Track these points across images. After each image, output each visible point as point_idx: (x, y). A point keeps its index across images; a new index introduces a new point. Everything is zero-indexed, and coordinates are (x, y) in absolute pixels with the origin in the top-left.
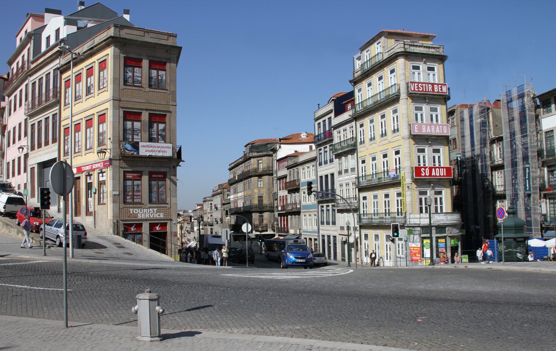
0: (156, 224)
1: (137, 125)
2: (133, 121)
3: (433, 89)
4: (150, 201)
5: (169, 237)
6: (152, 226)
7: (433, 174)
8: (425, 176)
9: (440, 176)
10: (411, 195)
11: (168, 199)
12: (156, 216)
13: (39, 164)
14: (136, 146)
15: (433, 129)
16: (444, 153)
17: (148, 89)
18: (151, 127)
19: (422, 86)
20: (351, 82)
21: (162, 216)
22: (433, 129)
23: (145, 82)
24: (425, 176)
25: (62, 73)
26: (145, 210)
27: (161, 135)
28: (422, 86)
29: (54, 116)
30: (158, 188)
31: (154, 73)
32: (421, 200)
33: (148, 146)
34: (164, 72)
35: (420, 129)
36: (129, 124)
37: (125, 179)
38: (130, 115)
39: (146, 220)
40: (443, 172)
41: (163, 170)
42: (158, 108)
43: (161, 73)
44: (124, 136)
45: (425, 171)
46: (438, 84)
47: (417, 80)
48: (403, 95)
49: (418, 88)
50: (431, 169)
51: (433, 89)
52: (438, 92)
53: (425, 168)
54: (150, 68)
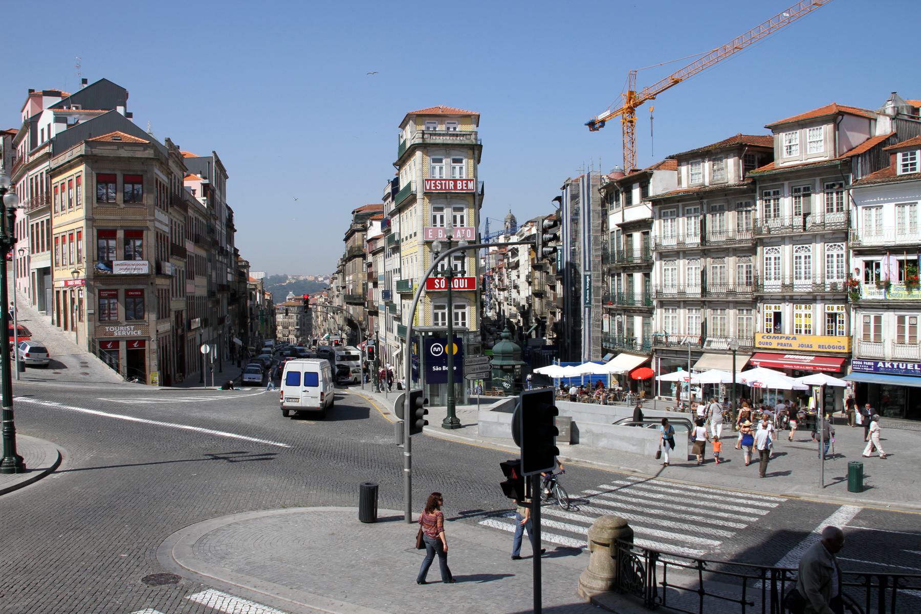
0: (134, 341)
1: (112, 243)
3: (455, 186)
4: (127, 319)
5: (147, 355)
6: (130, 343)
8: (440, 288)
9: (459, 288)
10: (424, 310)
11: (146, 316)
12: (134, 333)
13: (39, 270)
14: (109, 265)
17: (122, 206)
18: (127, 243)
19: (441, 184)
20: (395, 164)
21: (139, 333)
24: (440, 288)
25: (52, 177)
26: (122, 328)
27: (138, 252)
28: (441, 184)
29: (48, 220)
30: (135, 305)
31: (129, 187)
32: (436, 315)
33: (122, 265)
34: (140, 186)
36: (103, 243)
37: (100, 297)
38: (105, 234)
39: (122, 338)
41: (140, 287)
43: (137, 186)
44: (101, 256)
45: (439, 283)
46: (462, 181)
47: (438, 177)
48: (419, 195)
51: (455, 186)
52: (462, 189)
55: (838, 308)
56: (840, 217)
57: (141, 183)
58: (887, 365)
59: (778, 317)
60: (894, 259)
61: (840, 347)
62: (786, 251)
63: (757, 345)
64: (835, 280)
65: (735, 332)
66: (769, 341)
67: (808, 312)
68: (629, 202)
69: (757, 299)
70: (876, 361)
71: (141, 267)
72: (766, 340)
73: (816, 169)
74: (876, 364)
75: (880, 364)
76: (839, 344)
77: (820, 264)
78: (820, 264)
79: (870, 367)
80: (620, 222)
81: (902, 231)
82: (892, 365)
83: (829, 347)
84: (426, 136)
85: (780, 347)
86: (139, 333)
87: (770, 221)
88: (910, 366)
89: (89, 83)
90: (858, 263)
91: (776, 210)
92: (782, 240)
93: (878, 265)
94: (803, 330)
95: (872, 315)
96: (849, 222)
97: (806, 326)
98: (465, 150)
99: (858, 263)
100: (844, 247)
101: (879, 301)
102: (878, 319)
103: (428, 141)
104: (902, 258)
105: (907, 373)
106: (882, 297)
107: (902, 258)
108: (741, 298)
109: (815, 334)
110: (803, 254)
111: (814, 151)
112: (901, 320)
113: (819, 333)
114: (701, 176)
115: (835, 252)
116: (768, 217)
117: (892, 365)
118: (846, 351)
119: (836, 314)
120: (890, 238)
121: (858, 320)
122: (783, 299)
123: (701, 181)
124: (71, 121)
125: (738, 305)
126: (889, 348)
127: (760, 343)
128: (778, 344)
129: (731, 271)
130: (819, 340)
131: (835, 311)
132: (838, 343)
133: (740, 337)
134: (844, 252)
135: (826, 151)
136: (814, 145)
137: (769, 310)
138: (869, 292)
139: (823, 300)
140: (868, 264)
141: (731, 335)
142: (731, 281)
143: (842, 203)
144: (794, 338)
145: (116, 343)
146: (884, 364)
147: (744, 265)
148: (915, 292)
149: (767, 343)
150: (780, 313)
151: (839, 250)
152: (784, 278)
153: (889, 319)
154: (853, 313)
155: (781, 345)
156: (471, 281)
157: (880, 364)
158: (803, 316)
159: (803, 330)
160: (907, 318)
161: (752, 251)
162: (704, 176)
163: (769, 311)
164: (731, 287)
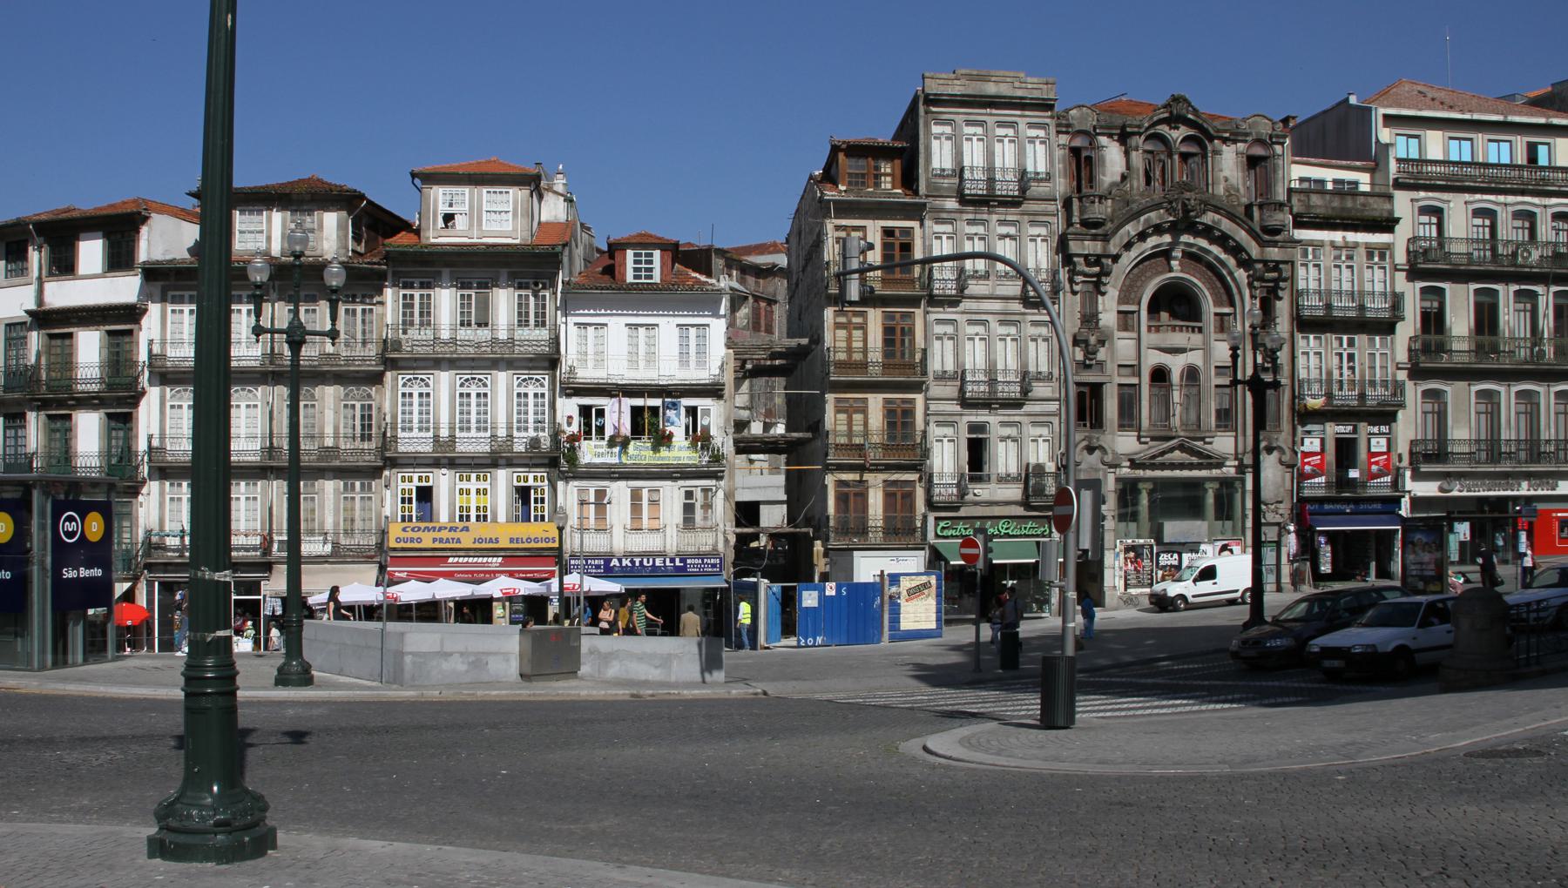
55: (535, 479)
56: (544, 334)
58: (626, 562)
59: (425, 494)
60: (628, 403)
61: (547, 540)
62: (444, 381)
63: (393, 544)
64: (532, 433)
65: (336, 524)
66: (415, 535)
67: (482, 485)
68: (64, 265)
69: (390, 460)
70: (607, 558)
72: (410, 534)
73: (506, 255)
74: (608, 562)
75: (615, 562)
76: (545, 535)
77: (507, 406)
78: (507, 406)
79: (598, 567)
80: (32, 306)
81: (633, 361)
82: (633, 562)
83: (529, 540)
85: (437, 545)
87: (413, 333)
88: (658, 562)
90: (568, 407)
91: (426, 312)
92: (437, 363)
93: (601, 413)
94: (473, 514)
95: (592, 486)
96: (555, 341)
97: (478, 509)
99: (568, 407)
100: (546, 383)
101: (611, 466)
102: (601, 494)
104: (639, 402)
105: (655, 572)
106: (615, 460)
107: (639, 402)
108: (352, 461)
109: (495, 520)
110: (473, 390)
111: (495, 227)
112: (636, 495)
113: (502, 517)
114: (263, 238)
115: (531, 390)
116: (408, 323)
117: (633, 562)
118: (556, 545)
119: (529, 488)
120: (618, 370)
121: (569, 493)
122: (436, 463)
123: (263, 246)
125: (345, 473)
126: (621, 539)
127: (398, 540)
128: (435, 540)
129: (329, 416)
130: (505, 529)
131: (531, 482)
132: (538, 532)
133: (349, 532)
134: (545, 390)
135: (515, 230)
136: (494, 216)
137: (405, 482)
138: (591, 452)
139: (510, 463)
140: (585, 411)
141: (329, 525)
142: (329, 430)
143: (544, 314)
144: (466, 529)
146: (620, 561)
147: (358, 405)
148: (664, 452)
149: (412, 540)
150: (430, 489)
151: (538, 386)
152: (437, 428)
153: (619, 492)
154: (560, 485)
155: (441, 540)
157: (615, 562)
158: (473, 492)
159: (473, 514)
160: (645, 493)
161: (376, 379)
162: (269, 239)
163: (407, 486)
164: (329, 442)
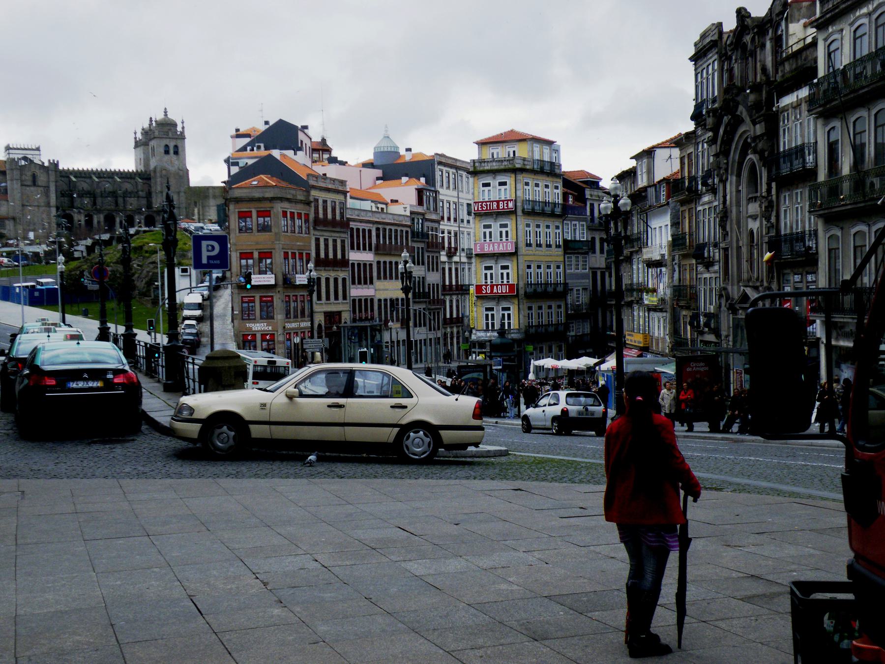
1: (250, 262)
2: (247, 259)
3: (498, 206)
4: (262, 318)
6: (263, 336)
7: (495, 291)
12: (266, 328)
15: (496, 247)
16: (512, 269)
21: (270, 328)
22: (496, 247)
23: (255, 228)
31: (261, 220)
32: (487, 316)
35: (482, 248)
36: (244, 262)
37: (243, 302)
40: (505, 290)
42: (265, 247)
43: (267, 219)
46: (503, 201)
49: (482, 207)
50: (492, 287)
51: (498, 206)
53: (486, 286)
54: (258, 216)
57: (269, 216)
71: (269, 279)
84: (477, 164)
86: (270, 328)
89: (271, 123)
98: (509, 174)
103: (478, 169)
124: (241, 165)
145: (254, 336)
156: (511, 287)
